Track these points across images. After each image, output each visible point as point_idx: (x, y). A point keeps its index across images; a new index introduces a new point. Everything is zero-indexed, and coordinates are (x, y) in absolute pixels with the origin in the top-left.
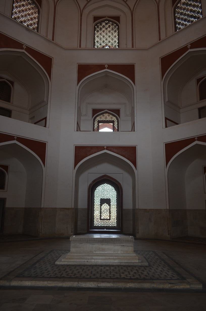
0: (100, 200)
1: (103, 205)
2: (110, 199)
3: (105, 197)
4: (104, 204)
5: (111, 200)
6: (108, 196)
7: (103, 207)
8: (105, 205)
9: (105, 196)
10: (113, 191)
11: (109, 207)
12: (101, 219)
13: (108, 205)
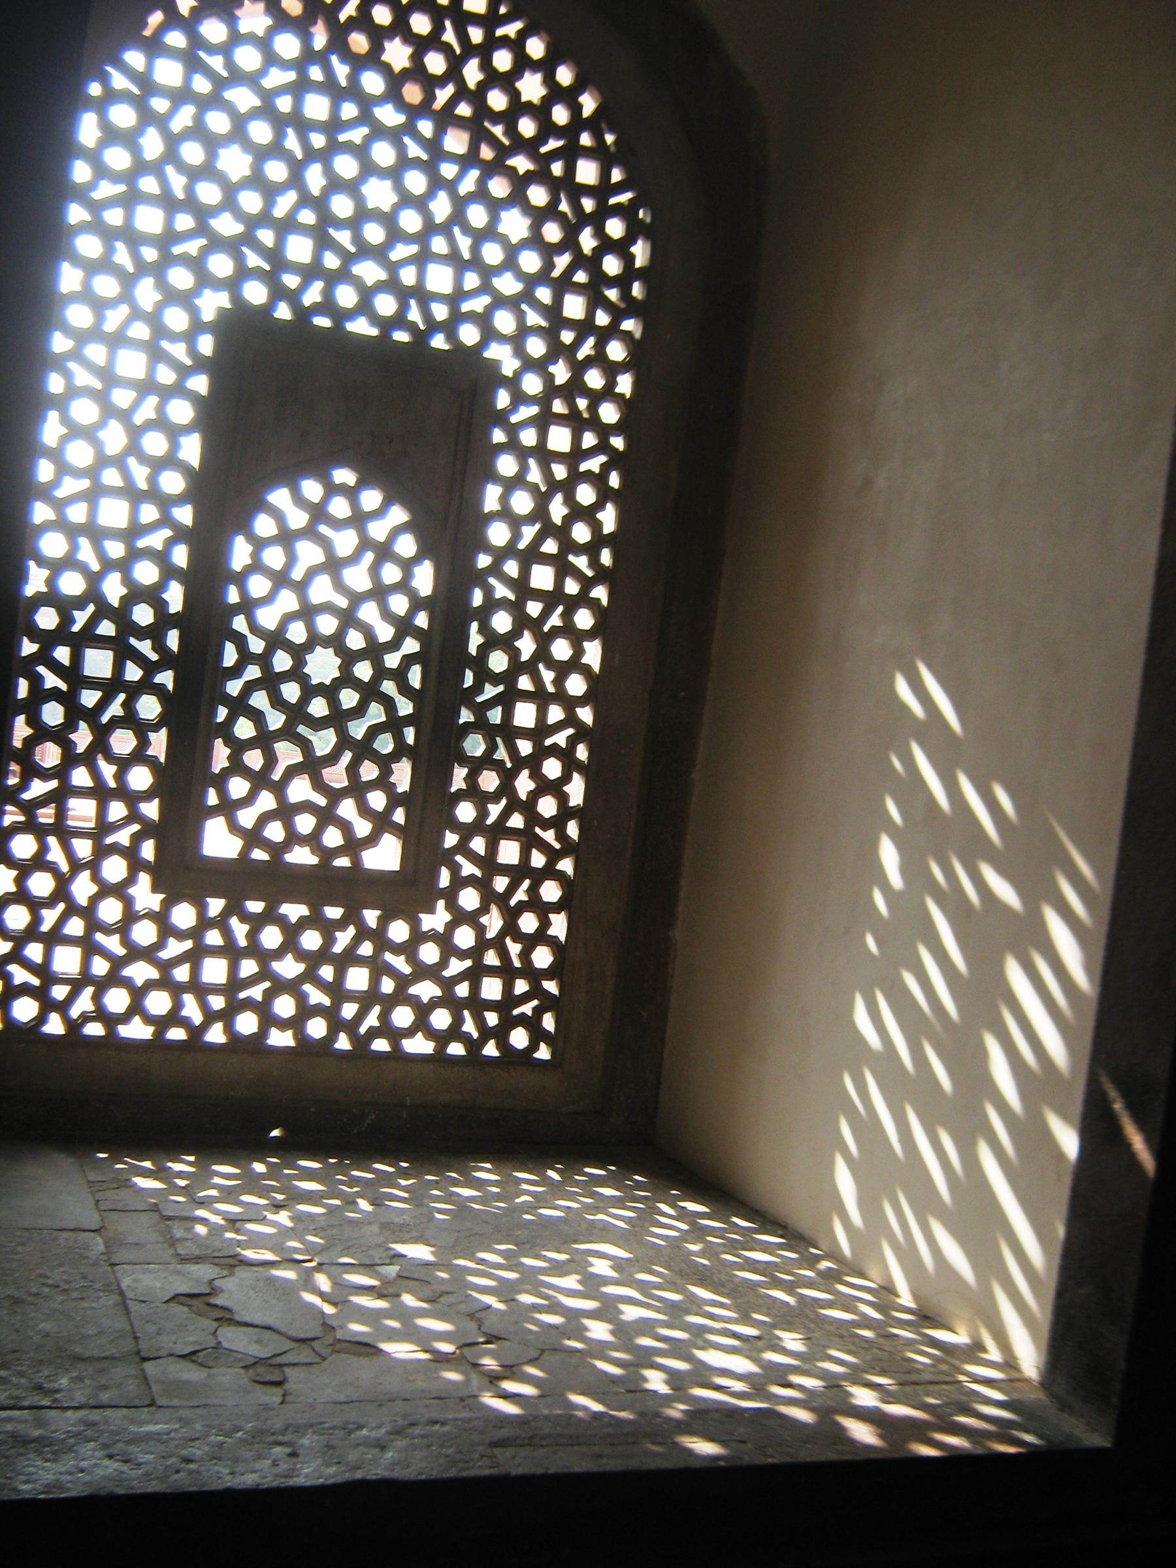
0: (206, 345)
1: (280, 497)
2: (492, 376)
3: (346, 297)
4: (312, 489)
5: (503, 399)
6: (440, 279)
7: (274, 557)
8: (340, 507)
9: (370, 272)
10: (587, 172)
11: (424, 579)
12: (182, 871)
13: (398, 515)
